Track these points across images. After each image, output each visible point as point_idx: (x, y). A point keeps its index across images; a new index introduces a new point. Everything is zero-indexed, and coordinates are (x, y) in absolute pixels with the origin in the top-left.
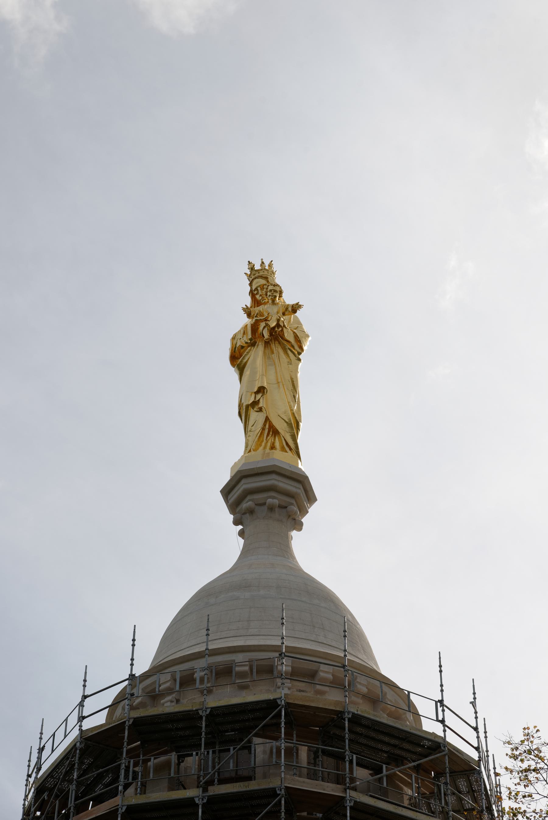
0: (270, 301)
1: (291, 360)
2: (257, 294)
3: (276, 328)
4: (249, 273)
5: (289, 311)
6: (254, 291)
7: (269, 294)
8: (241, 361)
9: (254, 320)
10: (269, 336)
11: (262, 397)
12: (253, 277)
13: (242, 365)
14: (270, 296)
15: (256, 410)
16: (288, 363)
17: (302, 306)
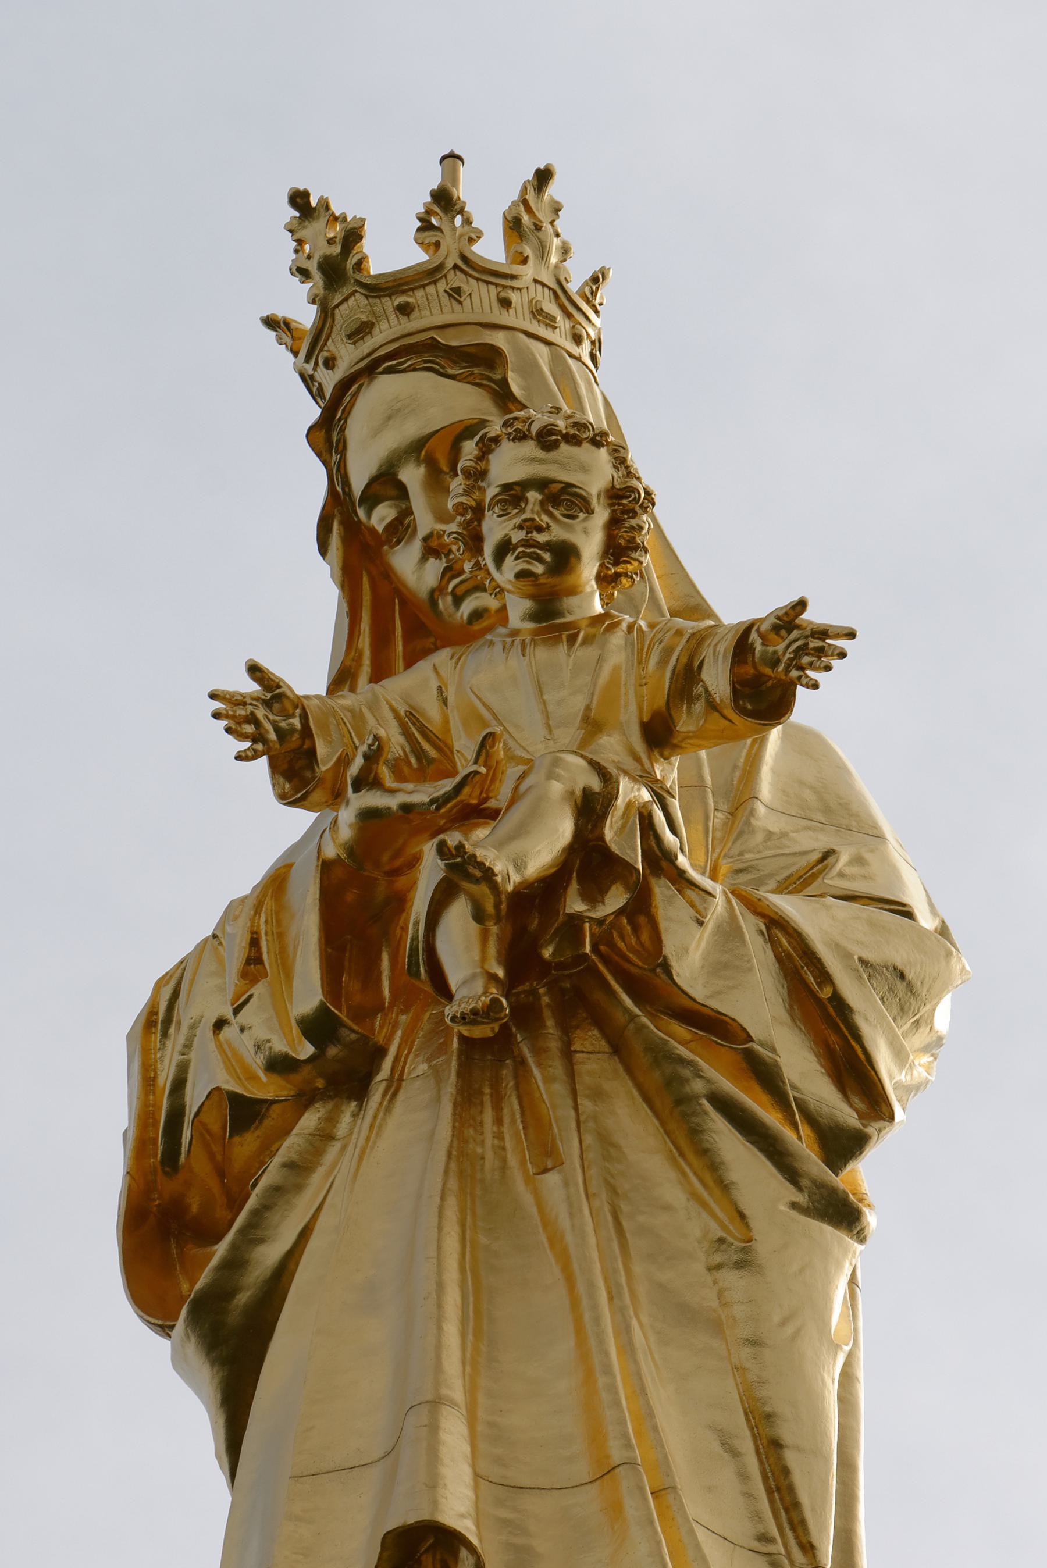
0: (518, 608)
3: (574, 887)
4: (306, 316)
5: (712, 706)
6: (371, 498)
8: (234, 1263)
9: (347, 816)
13: (243, 1298)
14: (503, 549)
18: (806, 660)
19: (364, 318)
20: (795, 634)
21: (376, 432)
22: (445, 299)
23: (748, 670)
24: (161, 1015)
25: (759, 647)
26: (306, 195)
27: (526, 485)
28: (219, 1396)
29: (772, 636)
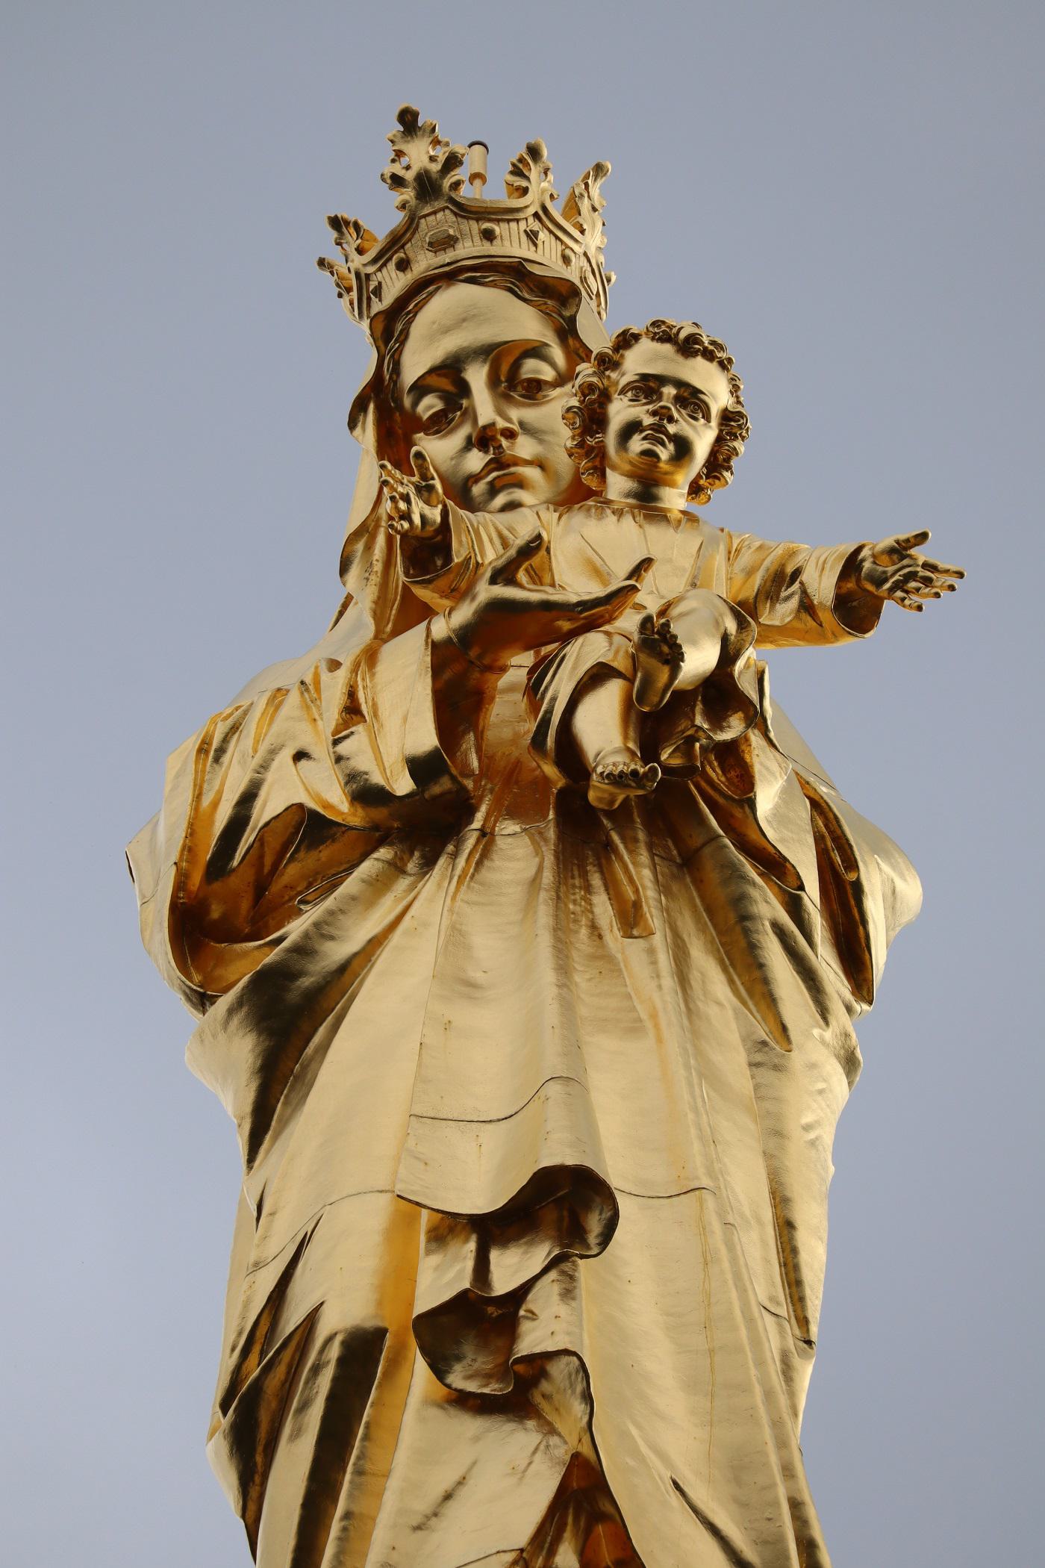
0: (618, 485)
1: (784, 1029)
2: (439, 424)
3: (699, 707)
5: (807, 606)
6: (420, 389)
7: (621, 411)
8: (304, 950)
10: (633, 753)
11: (553, 1275)
12: (424, 262)
13: (306, 982)
14: (632, 428)
15: (472, 1387)
16: (758, 1057)
17: (953, 580)
18: (913, 584)
19: (451, 232)
20: (905, 562)
21: (446, 330)
22: (524, 238)
23: (851, 585)
24: (215, 744)
25: (867, 565)
26: (415, 115)
27: (662, 380)
28: (259, 1063)
29: (885, 558)
